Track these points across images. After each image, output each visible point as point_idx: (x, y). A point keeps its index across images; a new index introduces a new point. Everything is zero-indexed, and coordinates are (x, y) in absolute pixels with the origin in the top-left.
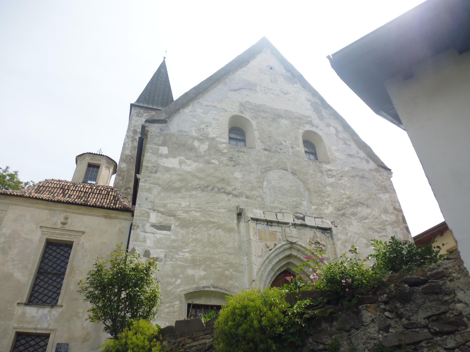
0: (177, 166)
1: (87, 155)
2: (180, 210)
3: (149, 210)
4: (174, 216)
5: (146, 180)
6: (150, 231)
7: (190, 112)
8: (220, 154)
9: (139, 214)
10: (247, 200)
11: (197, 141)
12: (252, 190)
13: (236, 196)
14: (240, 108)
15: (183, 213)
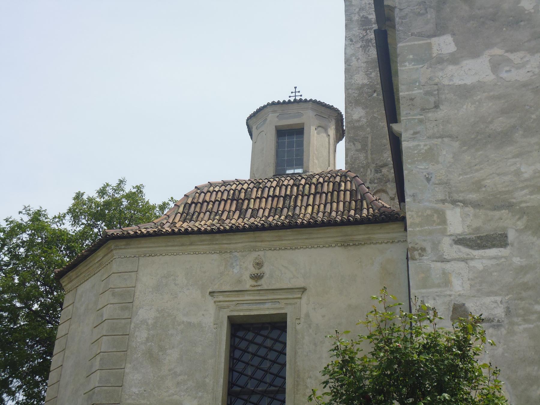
0: (487, 76)
1: (269, 109)
2: (523, 189)
3: (440, 206)
4: (510, 206)
5: (415, 133)
6: (455, 255)
9: (417, 220)
15: (531, 193)
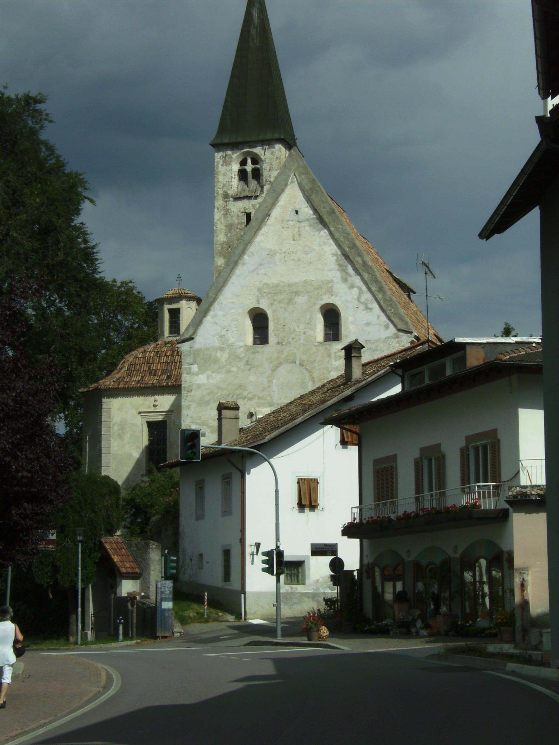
0: (205, 381)
3: (190, 424)
4: (207, 425)
5: (185, 400)
7: (212, 318)
8: (238, 360)
10: (259, 401)
11: (219, 351)
12: (263, 391)
13: (250, 399)
14: (258, 296)
